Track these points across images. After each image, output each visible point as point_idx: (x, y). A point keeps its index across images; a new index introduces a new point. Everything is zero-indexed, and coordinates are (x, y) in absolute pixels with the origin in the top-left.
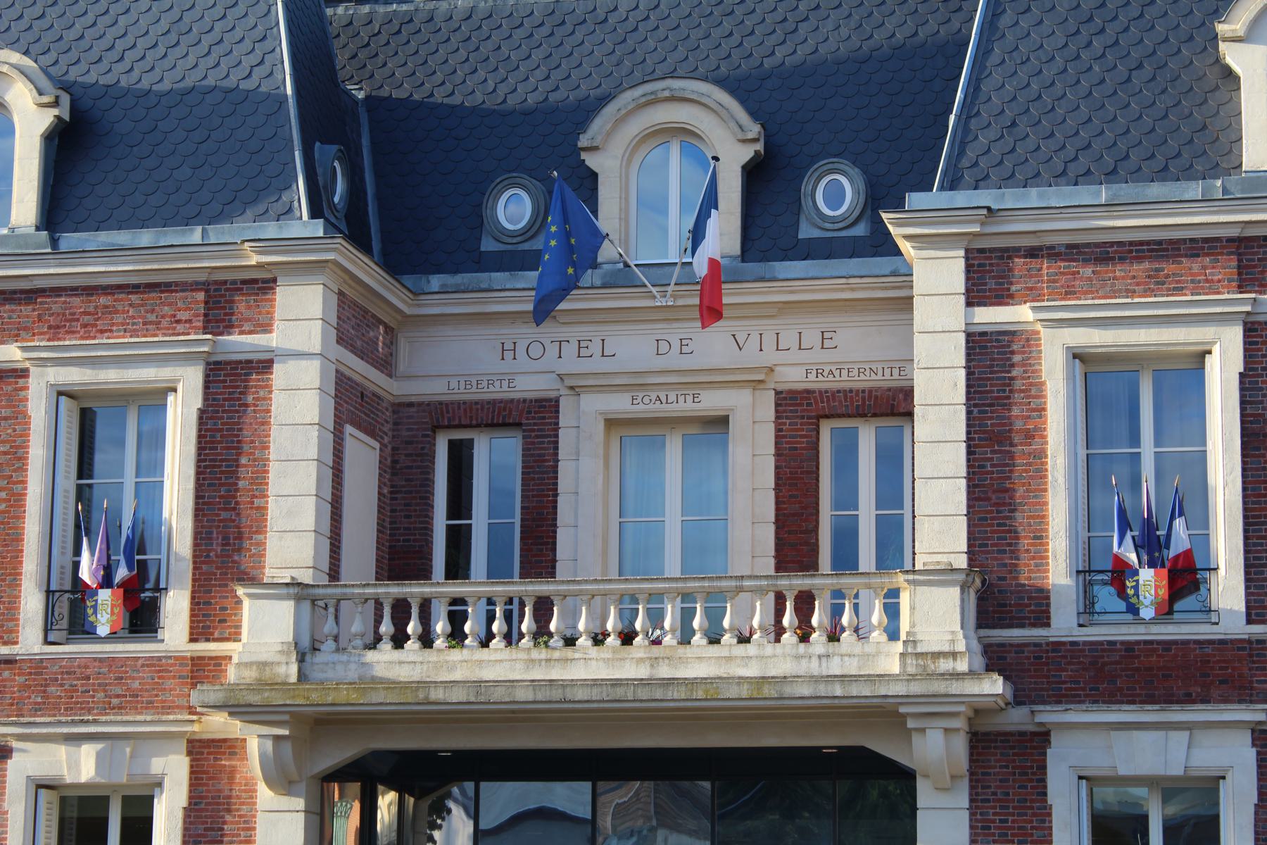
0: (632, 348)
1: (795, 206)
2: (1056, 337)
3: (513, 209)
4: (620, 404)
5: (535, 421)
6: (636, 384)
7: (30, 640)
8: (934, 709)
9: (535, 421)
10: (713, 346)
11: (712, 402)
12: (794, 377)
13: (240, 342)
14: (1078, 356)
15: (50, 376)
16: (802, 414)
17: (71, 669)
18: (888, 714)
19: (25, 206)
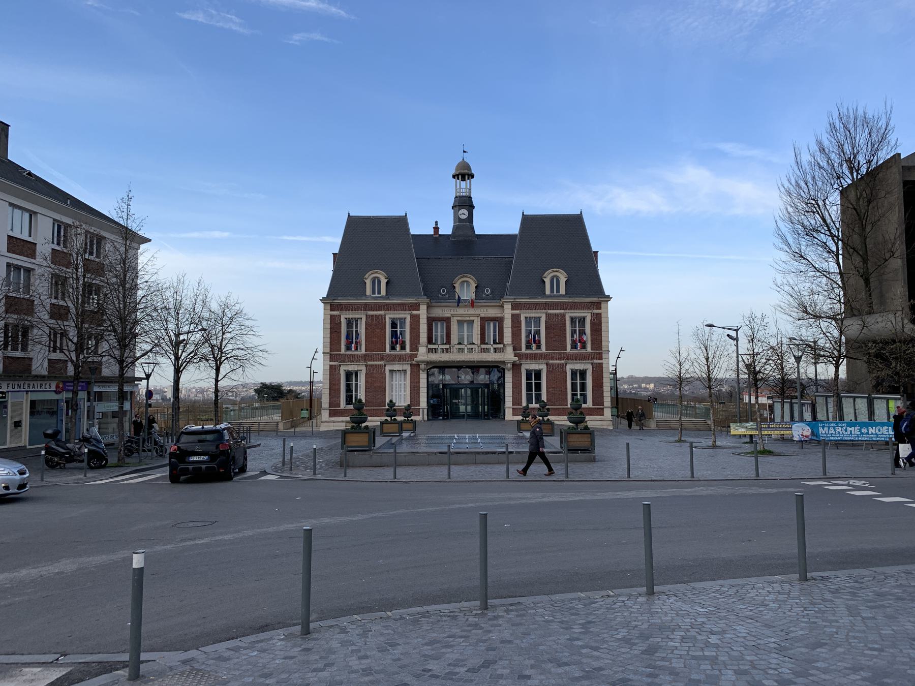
0: (461, 311)
1: (483, 292)
2: (524, 315)
3: (443, 291)
4: (459, 318)
5: (447, 321)
6: (461, 316)
7: (388, 351)
8: (509, 362)
9: (447, 321)
10: (471, 311)
11: (472, 318)
12: (482, 315)
13: (415, 312)
14: (526, 318)
15: (389, 317)
16: (484, 321)
17: (395, 356)
18: (504, 362)
19: (383, 293)
